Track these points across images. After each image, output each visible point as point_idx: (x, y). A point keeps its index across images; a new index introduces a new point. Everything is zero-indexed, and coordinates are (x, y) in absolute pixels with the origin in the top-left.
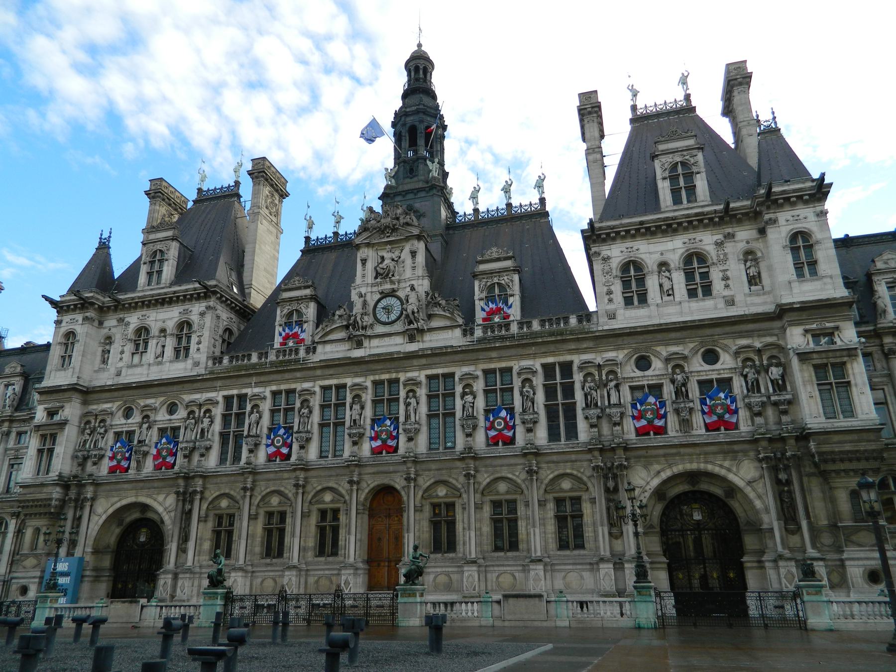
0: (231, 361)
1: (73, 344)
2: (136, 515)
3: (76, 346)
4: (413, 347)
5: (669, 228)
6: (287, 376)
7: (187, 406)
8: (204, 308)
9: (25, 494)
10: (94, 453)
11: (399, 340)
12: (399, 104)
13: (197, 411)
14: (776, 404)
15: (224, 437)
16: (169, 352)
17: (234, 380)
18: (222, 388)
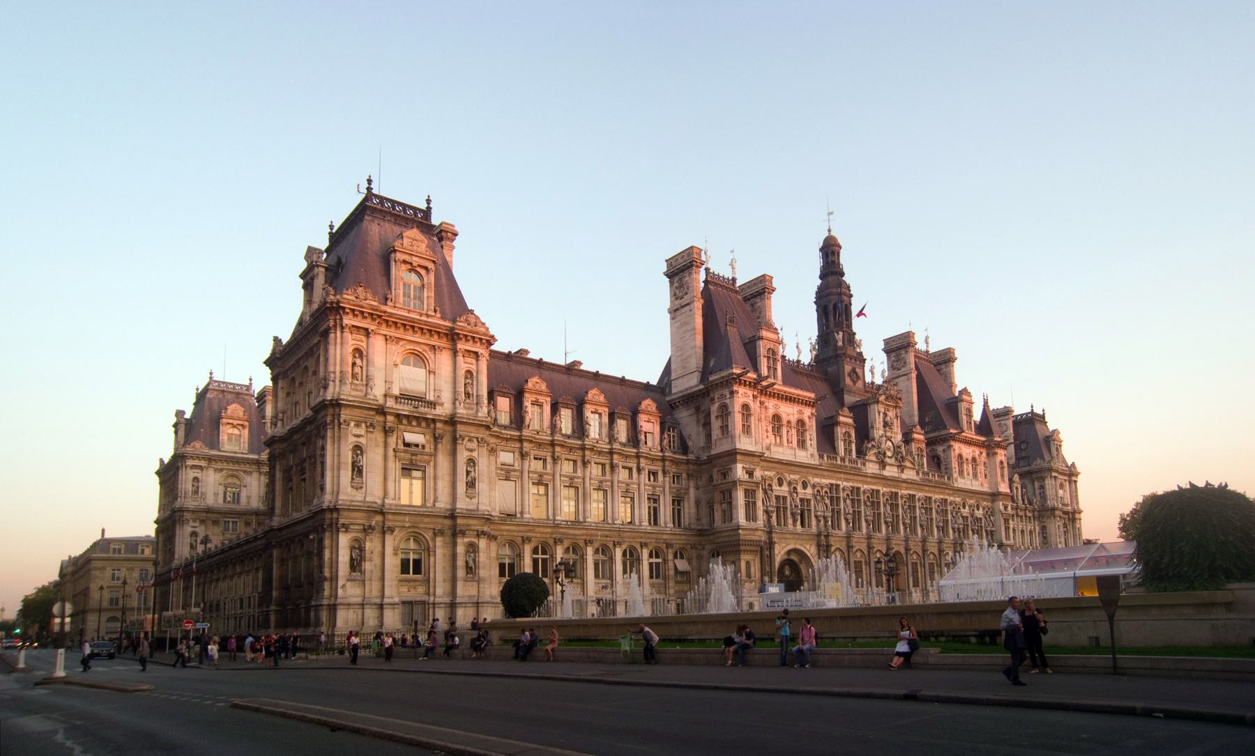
0: (828, 459)
1: (749, 415)
2: (786, 557)
3: (753, 418)
4: (904, 476)
5: (968, 442)
6: (856, 478)
7: (814, 486)
8: (810, 414)
9: (745, 535)
10: (771, 509)
11: (895, 469)
12: (819, 282)
13: (820, 490)
14: (992, 532)
15: (833, 510)
16: (795, 443)
17: (832, 473)
18: (829, 477)
